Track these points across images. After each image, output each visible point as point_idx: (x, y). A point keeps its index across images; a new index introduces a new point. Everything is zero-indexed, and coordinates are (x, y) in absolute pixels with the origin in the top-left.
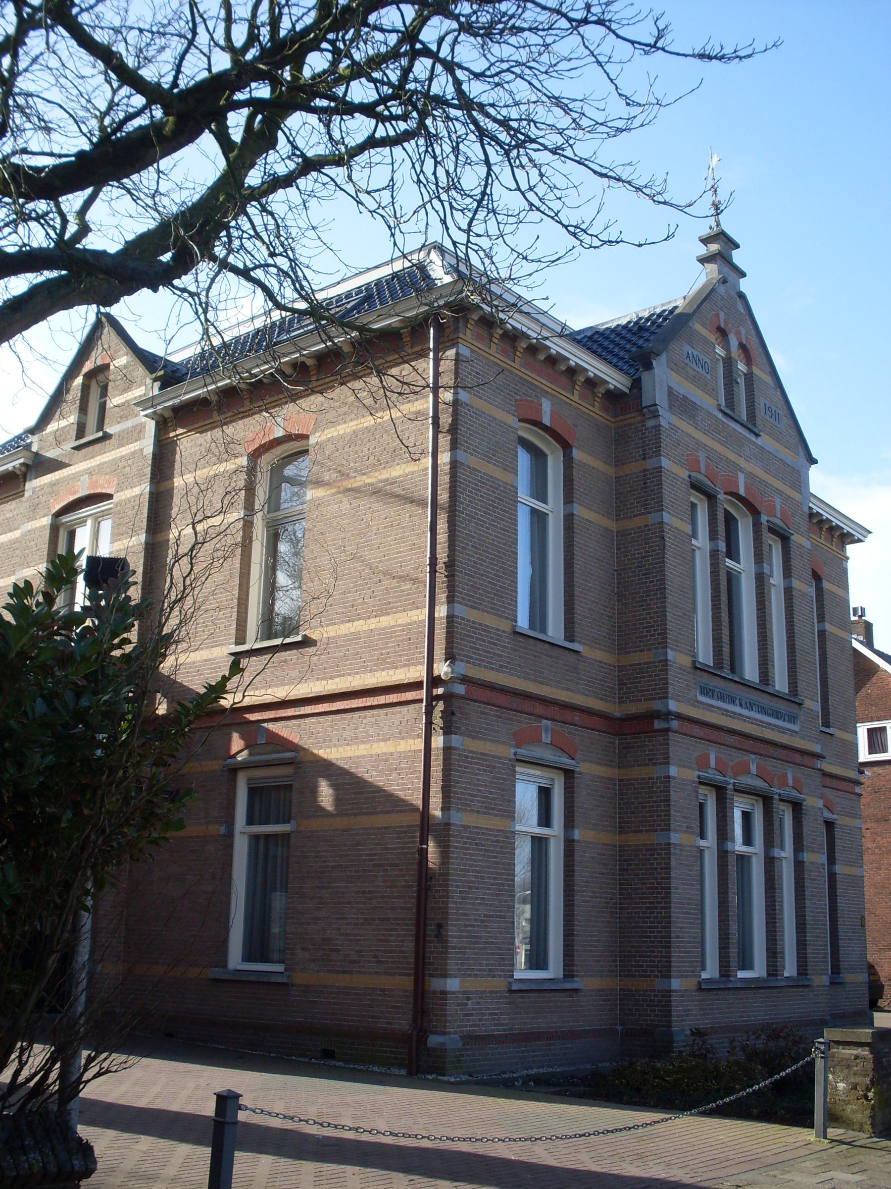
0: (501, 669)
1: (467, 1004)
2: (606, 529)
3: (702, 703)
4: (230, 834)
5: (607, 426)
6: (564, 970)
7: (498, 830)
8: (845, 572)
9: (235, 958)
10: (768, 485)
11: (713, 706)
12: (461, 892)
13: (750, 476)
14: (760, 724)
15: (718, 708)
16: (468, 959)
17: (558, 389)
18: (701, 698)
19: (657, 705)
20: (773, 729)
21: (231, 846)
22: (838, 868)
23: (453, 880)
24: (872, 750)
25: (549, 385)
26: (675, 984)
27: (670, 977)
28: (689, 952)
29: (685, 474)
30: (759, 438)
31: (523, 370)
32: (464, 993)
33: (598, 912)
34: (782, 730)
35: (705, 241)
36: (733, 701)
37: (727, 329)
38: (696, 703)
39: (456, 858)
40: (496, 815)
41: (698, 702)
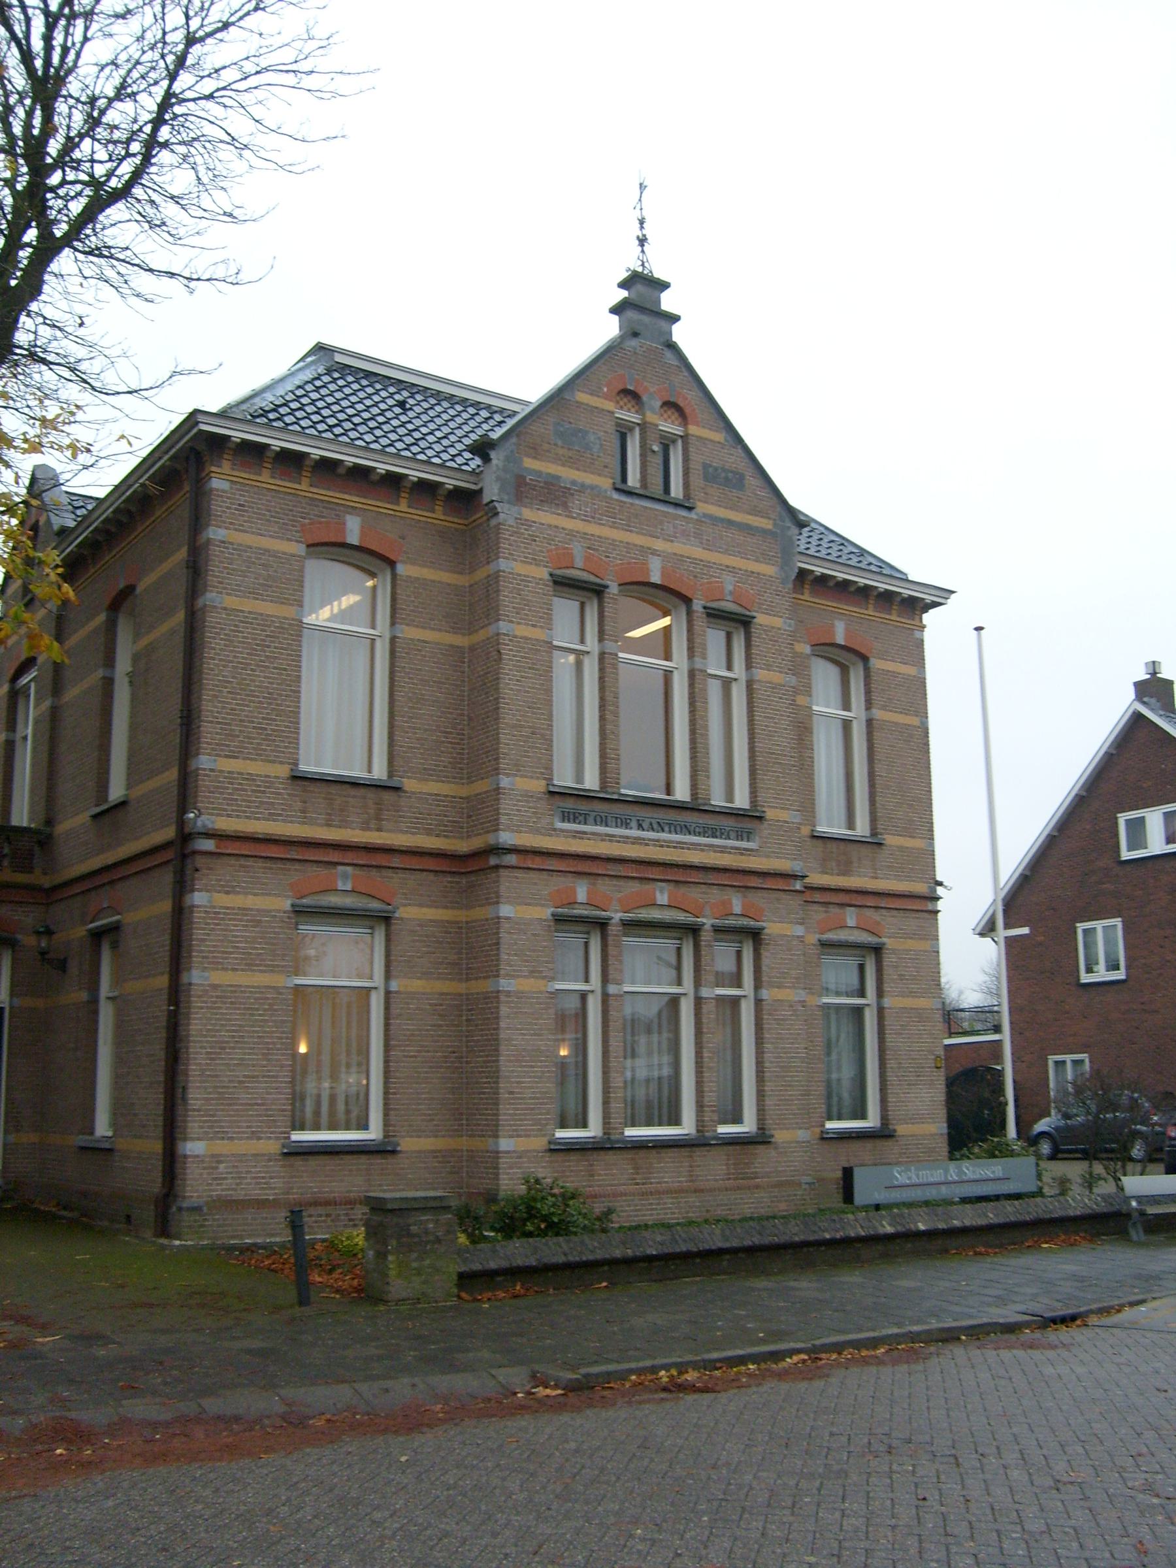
0: (271, 817)
1: (217, 1168)
2: (451, 646)
3: (562, 831)
4: (94, 1001)
5: (456, 530)
6: (385, 1131)
7: (266, 987)
8: (920, 644)
9: (103, 1127)
10: (708, 565)
11: (585, 833)
12: (208, 1053)
13: (665, 556)
14: (679, 845)
15: (593, 834)
16: (220, 1121)
17: (373, 503)
18: (560, 825)
19: (491, 839)
20: (702, 850)
21: (96, 1012)
22: (887, 1002)
23: (195, 1042)
24: (1131, 848)
25: (357, 499)
26: (505, 1144)
27: (497, 1137)
28: (532, 1109)
29: (543, 573)
30: (694, 512)
31: (315, 490)
32: (213, 1156)
33: (431, 1067)
34: (723, 850)
35: (623, 285)
36: (626, 825)
37: (639, 391)
38: (553, 831)
39: (200, 1019)
40: (261, 971)
41: (555, 830)
